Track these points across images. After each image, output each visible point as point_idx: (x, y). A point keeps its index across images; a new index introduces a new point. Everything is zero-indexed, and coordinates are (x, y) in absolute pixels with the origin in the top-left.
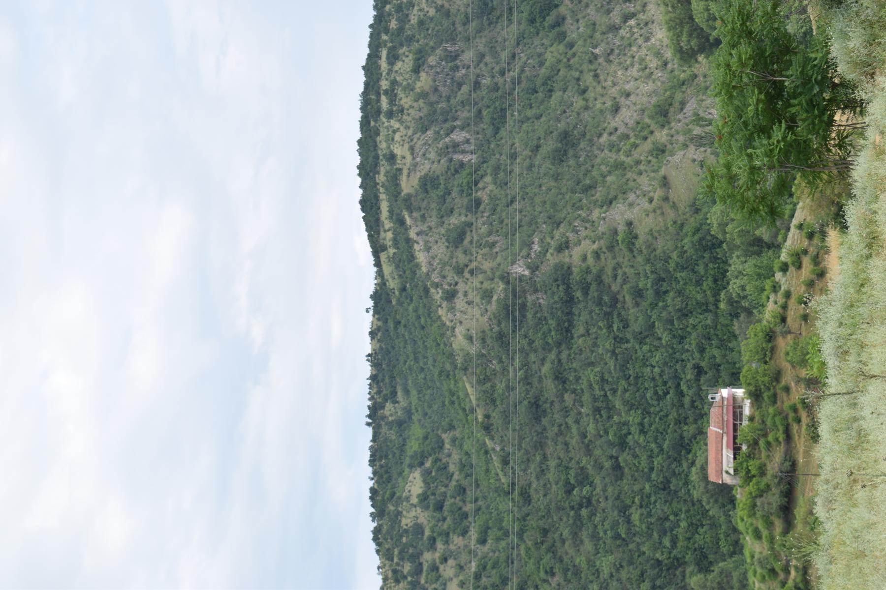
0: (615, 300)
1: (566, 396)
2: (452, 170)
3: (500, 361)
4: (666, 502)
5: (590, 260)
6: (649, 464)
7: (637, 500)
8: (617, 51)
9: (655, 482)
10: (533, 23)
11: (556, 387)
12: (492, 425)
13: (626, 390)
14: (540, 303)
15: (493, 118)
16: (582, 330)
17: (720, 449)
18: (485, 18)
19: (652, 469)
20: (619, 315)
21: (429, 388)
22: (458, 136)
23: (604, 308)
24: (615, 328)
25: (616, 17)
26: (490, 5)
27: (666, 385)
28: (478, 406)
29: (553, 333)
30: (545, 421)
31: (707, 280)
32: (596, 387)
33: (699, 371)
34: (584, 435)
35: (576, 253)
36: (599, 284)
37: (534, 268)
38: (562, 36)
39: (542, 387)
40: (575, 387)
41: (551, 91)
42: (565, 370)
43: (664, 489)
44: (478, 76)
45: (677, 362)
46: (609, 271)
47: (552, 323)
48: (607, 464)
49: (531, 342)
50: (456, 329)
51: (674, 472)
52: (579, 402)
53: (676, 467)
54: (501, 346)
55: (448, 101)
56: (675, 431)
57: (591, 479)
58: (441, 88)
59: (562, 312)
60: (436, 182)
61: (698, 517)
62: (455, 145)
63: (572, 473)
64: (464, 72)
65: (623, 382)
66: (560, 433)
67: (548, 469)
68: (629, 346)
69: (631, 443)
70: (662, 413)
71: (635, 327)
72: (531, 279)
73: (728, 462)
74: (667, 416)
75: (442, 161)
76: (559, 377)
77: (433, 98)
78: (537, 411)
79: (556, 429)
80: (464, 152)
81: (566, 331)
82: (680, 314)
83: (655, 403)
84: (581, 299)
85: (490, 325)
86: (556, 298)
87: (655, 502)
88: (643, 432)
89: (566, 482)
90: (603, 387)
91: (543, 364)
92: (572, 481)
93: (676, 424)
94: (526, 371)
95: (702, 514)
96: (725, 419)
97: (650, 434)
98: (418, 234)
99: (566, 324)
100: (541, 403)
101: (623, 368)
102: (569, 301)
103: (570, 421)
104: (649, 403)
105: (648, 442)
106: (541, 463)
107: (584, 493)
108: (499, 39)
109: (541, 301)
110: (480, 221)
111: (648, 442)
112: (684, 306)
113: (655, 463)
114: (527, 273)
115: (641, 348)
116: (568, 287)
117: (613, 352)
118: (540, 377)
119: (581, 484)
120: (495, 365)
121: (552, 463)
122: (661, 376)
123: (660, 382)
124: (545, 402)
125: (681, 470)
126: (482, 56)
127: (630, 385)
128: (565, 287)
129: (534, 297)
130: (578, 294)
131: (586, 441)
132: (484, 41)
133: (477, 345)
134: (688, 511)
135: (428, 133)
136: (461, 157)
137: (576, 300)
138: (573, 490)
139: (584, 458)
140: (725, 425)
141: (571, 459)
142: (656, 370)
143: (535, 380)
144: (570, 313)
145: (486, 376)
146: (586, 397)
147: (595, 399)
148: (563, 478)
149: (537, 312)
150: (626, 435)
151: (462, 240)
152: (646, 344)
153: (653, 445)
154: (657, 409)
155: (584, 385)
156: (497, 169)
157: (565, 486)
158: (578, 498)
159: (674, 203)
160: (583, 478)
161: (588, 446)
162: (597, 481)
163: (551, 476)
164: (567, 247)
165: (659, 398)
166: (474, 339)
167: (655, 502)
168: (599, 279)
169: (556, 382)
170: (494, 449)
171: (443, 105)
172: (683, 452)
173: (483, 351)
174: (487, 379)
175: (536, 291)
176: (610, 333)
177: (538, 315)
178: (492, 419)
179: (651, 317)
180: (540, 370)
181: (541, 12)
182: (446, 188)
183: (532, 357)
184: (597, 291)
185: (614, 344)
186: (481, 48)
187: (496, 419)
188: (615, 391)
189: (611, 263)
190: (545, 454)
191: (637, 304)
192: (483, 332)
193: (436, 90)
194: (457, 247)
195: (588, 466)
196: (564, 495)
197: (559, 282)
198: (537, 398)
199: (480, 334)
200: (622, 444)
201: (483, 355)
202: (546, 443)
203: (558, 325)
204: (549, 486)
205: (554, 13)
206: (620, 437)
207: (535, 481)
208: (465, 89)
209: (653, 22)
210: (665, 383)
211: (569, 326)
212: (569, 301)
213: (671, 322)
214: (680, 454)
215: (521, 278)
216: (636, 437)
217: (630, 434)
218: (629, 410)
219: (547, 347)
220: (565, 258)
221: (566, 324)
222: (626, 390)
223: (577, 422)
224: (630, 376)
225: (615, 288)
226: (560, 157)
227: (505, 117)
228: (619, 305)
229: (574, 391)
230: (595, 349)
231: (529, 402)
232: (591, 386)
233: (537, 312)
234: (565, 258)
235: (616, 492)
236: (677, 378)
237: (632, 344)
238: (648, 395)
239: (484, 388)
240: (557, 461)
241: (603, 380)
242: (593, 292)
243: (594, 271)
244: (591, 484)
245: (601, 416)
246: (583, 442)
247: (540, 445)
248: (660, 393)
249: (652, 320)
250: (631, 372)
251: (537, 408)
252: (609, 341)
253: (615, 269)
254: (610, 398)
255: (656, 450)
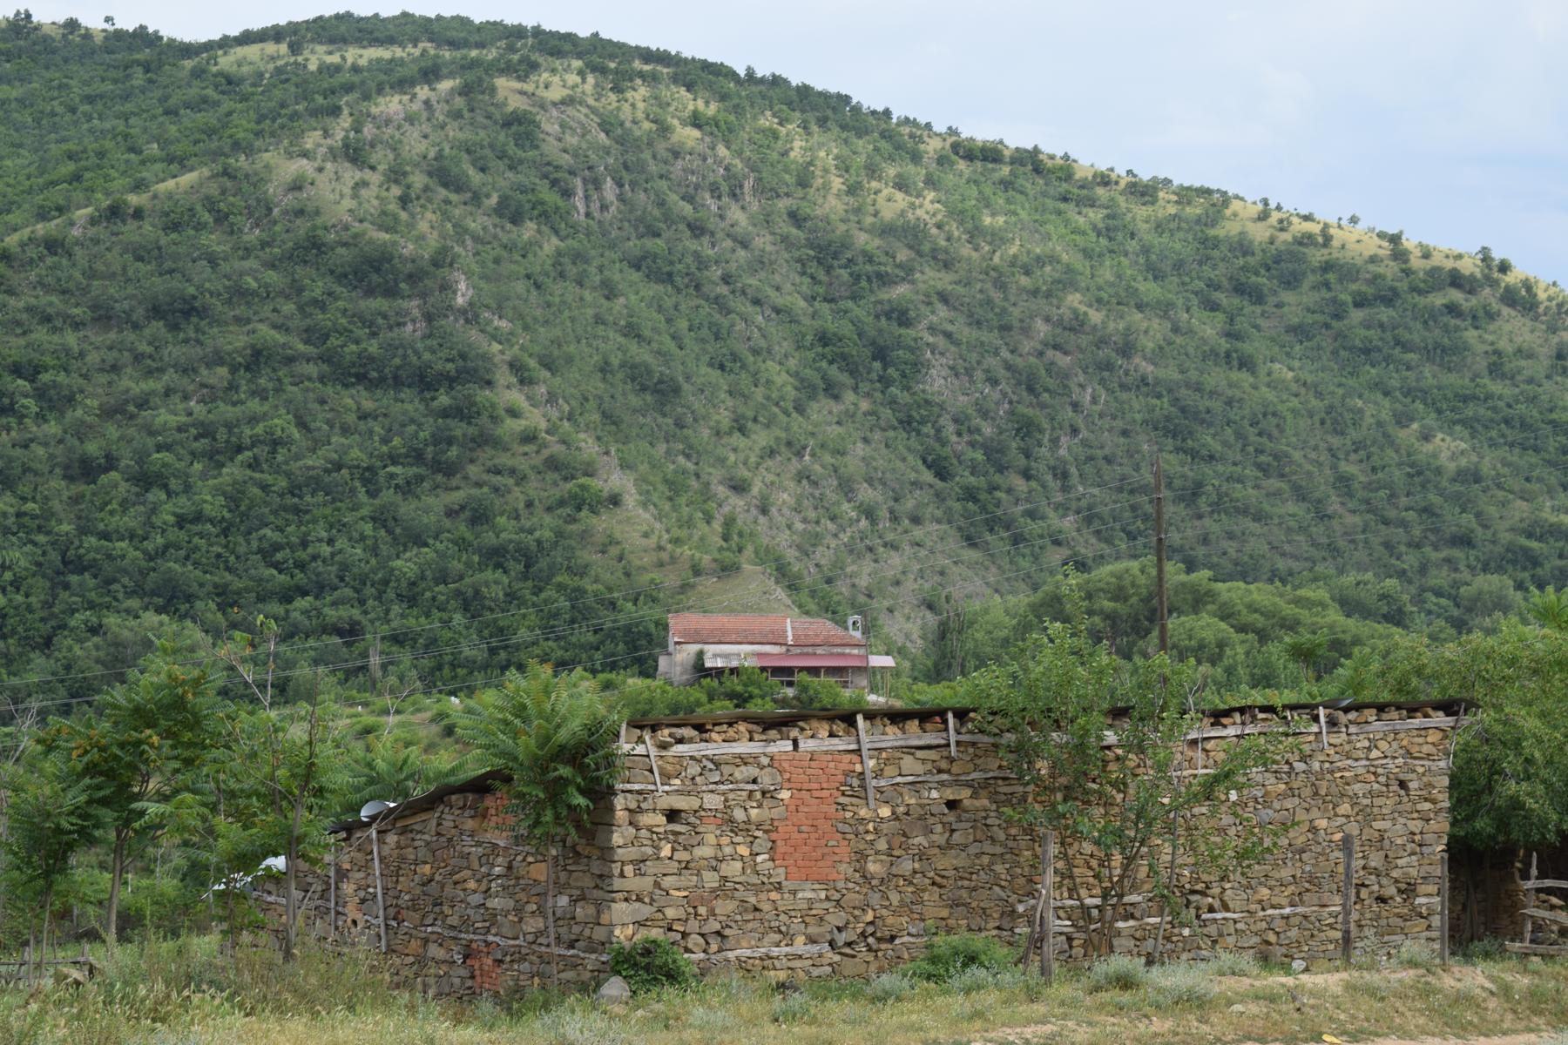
0: (449, 470)
1: (223, 371)
2: (558, 175)
3: (264, 244)
4: (39, 564)
5: (517, 425)
6: (117, 531)
7: (30, 506)
8: (817, 493)
9: (77, 543)
10: (820, 340)
11: (236, 351)
12: (124, 222)
13: (265, 488)
14: (404, 324)
15: (655, 256)
16: (368, 405)
17: (750, 639)
18: (812, 253)
19: (105, 536)
20: (420, 479)
21: (37, 121)
22: (609, 190)
23: (430, 449)
24: (391, 469)
25: (866, 493)
26: (836, 263)
27: (296, 566)
28: (155, 197)
29: (354, 347)
30: (157, 327)
31: (560, 648)
32: (259, 429)
33: (350, 632)
34: (143, 403)
35: (516, 397)
36: (473, 440)
37: (470, 315)
38: (808, 390)
39: (226, 323)
40: (244, 388)
41: (722, 367)
42: (274, 370)
43: (65, 562)
44: (712, 234)
45: (357, 591)
46: (504, 460)
47: (373, 347)
48: (92, 448)
49: (322, 307)
50: (305, 161)
51: (115, 580)
52: (211, 396)
53: (124, 587)
54: (297, 246)
55: (661, 177)
56: (201, 585)
57: (51, 416)
58: (680, 163)
59: (398, 368)
60: (528, 143)
61: (20, 629)
62: (597, 184)
63: (62, 378)
64: (714, 208)
65: (283, 483)
66: (138, 358)
67: (55, 330)
68: (362, 496)
69: (150, 497)
70: (232, 558)
71: (406, 508)
72: (450, 307)
73: (726, 656)
74: (228, 569)
75: (567, 156)
76: (257, 358)
77: (661, 147)
78: (174, 312)
79: (144, 347)
80: (587, 198)
81: (359, 374)
82: (470, 593)
83: (255, 544)
84: (435, 404)
85: (334, 226)
86: (427, 356)
87: (35, 544)
88: (181, 521)
89: (36, 366)
90: (261, 442)
91: (275, 327)
92: (45, 377)
93: (216, 586)
94: (254, 293)
95: (27, 638)
96: (819, 651)
97: (183, 535)
98: (427, 103)
99: (375, 374)
100: (194, 319)
101: (315, 484)
102: (425, 382)
103: (170, 377)
104: (250, 533)
105: (164, 531)
106: (66, 317)
107: (25, 401)
108: (777, 278)
109: (410, 327)
110: (486, 220)
111: (164, 531)
112: (487, 603)
113: (123, 544)
114: (460, 300)
115: (362, 519)
116: (451, 381)
117: (338, 467)
118: (248, 321)
119: (41, 394)
120: (252, 236)
121: (71, 339)
122: (314, 558)
123: (302, 555)
124: (197, 330)
125: (120, 596)
126: (745, 245)
127: (281, 495)
128: (453, 373)
129: (416, 313)
130: (444, 400)
131: (131, 408)
132: (769, 248)
133: (289, 200)
134: (30, 609)
135: (603, 135)
136: (580, 193)
137: (428, 395)
138: (26, 379)
139: (96, 403)
140: (806, 650)
141: (85, 377)
142: (326, 550)
143: (241, 311)
144: (398, 383)
145: (227, 216)
146: (226, 411)
147: (230, 426)
148: (48, 359)
149: (385, 317)
150: (165, 487)
151: (445, 185)
152: (375, 529)
153: (160, 540)
154: (242, 549)
155: (254, 405)
156: (578, 257)
157: (30, 361)
158: (11, 387)
159: (693, 586)
160: (51, 400)
161: (123, 412)
162: (52, 428)
163: (41, 334)
164: (522, 382)
165: (267, 553)
166: (297, 194)
167: (35, 544)
168: (484, 440)
169: (249, 351)
170: (72, 224)
171: (653, 168)
172: (160, 601)
173: (276, 211)
174: (221, 218)
175: (429, 318)
176: (381, 457)
177: (380, 321)
178: (136, 224)
179: (436, 537)
180: (261, 321)
181: (844, 357)
182: (521, 162)
183: (289, 308)
184: (464, 435)
185: (358, 467)
186: (758, 242)
187: (130, 231)
188: (254, 465)
189: (522, 464)
190: (84, 325)
191: (450, 513)
192: (317, 213)
193: (676, 154)
194: (430, 174)
195: (79, 412)
196: (10, 360)
197: (461, 363)
198: (202, 313)
199: (310, 207)
200: (146, 480)
201: (270, 210)
202: (108, 329)
203: (372, 359)
204: (19, 331)
205: (845, 378)
206: (159, 476)
207: (21, 304)
208: (687, 209)
209: (876, 561)
210: (301, 566)
211: (370, 381)
212: (425, 382)
213: (443, 578)
214: (153, 593)
215: (447, 287)
216: (169, 507)
217: (169, 495)
218: (224, 494)
219: (313, 335)
220: (503, 377)
221: (375, 374)
222: (265, 488)
223: (168, 393)
224: (301, 497)
225: (473, 470)
226: (638, 376)
227: (659, 281)
228: (439, 478)
229: (232, 387)
230: (337, 430)
231: (194, 298)
232: (253, 420)
233: (385, 317)
234: (503, 377)
235: (36, 465)
236: (320, 589)
237: (367, 506)
238: (267, 532)
239: (199, 208)
240: (76, 349)
241: (276, 443)
242: (459, 429)
243: (499, 431)
244: (41, 418)
245: (196, 439)
246: (127, 402)
247: (103, 316)
248: (279, 556)
249: (431, 541)
250: (308, 498)
251: (181, 311)
252: (364, 457)
253: (512, 471)
254: (240, 457)
255: (149, 546)
